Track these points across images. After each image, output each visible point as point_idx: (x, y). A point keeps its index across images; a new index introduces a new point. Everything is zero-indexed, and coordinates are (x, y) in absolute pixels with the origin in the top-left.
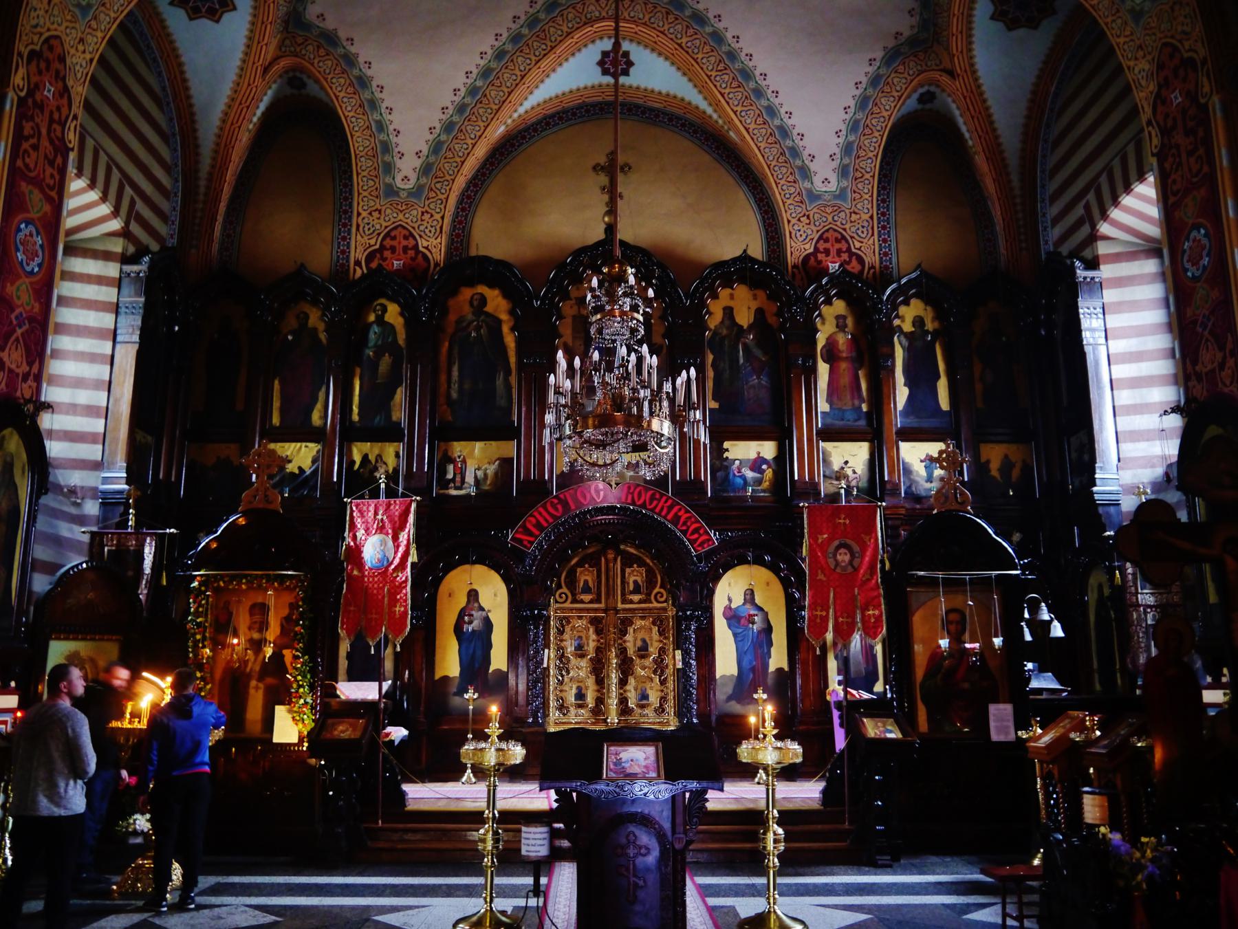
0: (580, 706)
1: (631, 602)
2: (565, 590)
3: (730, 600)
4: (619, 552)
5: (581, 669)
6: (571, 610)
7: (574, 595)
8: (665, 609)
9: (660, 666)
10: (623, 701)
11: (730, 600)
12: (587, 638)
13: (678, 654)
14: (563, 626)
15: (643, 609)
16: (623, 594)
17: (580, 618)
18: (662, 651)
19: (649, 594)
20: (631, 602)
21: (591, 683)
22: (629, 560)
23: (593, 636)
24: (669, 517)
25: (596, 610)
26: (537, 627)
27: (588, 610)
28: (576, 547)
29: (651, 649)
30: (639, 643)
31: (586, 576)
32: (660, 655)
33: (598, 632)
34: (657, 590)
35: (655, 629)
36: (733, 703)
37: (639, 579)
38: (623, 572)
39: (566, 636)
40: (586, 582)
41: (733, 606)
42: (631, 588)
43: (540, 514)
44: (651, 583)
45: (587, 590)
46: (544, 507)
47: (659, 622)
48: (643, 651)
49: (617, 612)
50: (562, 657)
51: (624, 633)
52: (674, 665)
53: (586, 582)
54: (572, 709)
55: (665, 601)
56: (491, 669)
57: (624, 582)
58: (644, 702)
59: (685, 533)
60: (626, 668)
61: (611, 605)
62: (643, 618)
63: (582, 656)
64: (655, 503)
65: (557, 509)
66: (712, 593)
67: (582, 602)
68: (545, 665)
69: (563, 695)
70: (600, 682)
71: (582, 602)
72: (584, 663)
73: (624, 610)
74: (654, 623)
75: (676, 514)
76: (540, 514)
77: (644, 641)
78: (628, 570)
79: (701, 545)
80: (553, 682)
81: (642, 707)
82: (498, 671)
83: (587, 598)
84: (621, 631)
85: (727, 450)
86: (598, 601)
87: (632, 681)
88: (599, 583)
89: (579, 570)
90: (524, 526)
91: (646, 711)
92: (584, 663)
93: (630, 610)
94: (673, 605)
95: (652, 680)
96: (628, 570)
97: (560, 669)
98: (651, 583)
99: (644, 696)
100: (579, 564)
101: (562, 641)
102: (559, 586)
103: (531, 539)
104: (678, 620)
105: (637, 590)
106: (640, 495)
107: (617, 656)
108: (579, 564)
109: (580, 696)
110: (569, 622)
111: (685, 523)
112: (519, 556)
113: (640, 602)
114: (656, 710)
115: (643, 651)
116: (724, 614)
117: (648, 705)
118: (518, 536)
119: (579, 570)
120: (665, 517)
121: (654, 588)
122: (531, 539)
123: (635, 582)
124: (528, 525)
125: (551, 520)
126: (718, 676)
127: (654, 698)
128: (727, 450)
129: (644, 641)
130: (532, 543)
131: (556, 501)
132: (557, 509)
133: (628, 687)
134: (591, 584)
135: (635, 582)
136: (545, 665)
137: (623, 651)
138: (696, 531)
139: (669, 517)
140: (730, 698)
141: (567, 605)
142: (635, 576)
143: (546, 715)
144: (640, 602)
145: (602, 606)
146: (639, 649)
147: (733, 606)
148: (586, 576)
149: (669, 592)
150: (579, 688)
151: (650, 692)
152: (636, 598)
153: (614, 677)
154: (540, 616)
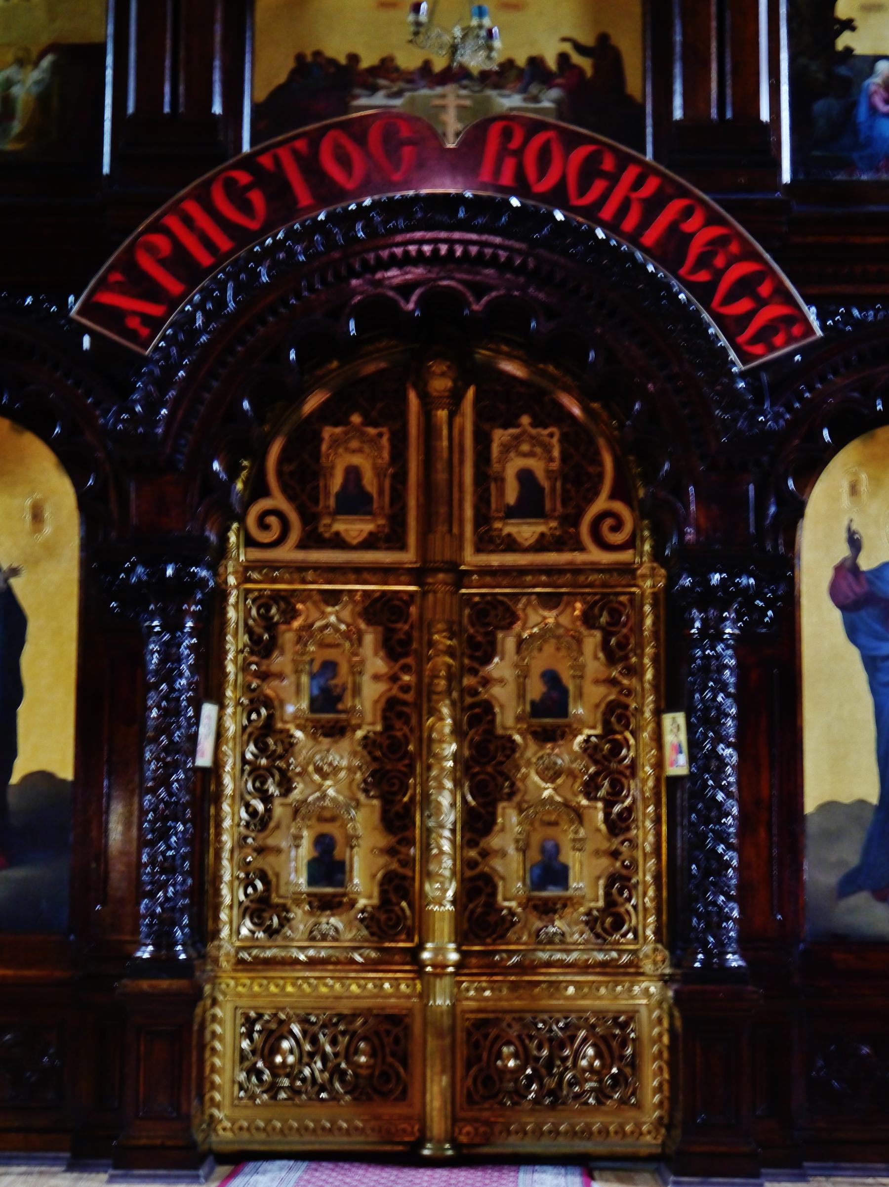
0: (326, 904)
1: (511, 545)
2: (278, 500)
3: (855, 543)
4: (468, 373)
5: (331, 772)
6: (300, 570)
7: (309, 518)
8: (628, 571)
9: (608, 768)
10: (477, 887)
11: (855, 543)
12: (357, 670)
13: (675, 727)
14: (270, 626)
15: (550, 570)
16: (482, 519)
17: (332, 598)
18: (616, 716)
19: (572, 520)
20: (511, 545)
21: (364, 823)
22: (501, 405)
23: (377, 664)
24: (650, 237)
25: (386, 573)
26: (173, 625)
27: (359, 572)
28: (322, 345)
29: (578, 710)
30: (536, 689)
31: (354, 457)
32: (608, 730)
33: (393, 648)
34: (601, 504)
35: (592, 641)
36: (862, 899)
37: (537, 466)
38: (482, 440)
39: (280, 661)
40: (353, 474)
41: (866, 563)
42: (511, 496)
43: (188, 221)
44: (578, 480)
45: (354, 501)
46: (203, 198)
47: (607, 612)
48: (550, 712)
49: (461, 578)
50: (265, 733)
51: (485, 651)
52: (659, 765)
53: (353, 474)
54: (299, 916)
55: (630, 544)
56: (20, 770)
57: (486, 478)
58: (551, 892)
59: (704, 293)
60: (489, 774)
61: (441, 551)
62: (550, 601)
63: (336, 731)
64: (599, 186)
65: (246, 208)
66: (794, 510)
67: (338, 543)
68: (204, 759)
69: (269, 863)
70: (401, 821)
71: (338, 543)
72: (341, 756)
73: (486, 572)
74: (588, 620)
75: (673, 228)
76: (188, 221)
77: (552, 678)
78: (500, 436)
79: (764, 336)
80: (231, 817)
81: (548, 910)
82: (42, 779)
83: (355, 528)
84: (473, 644)
85: (849, 25)
86: (393, 538)
87: (509, 818)
88: (400, 479)
89: (328, 432)
90: (128, 265)
91: (559, 925)
92: (341, 756)
93: (504, 572)
94: (657, 555)
95: (579, 816)
96: (500, 436)
97: (259, 775)
98: (578, 480)
99: (550, 872)
100: (330, 414)
101: (264, 676)
102: (257, 489)
103: (155, 310)
104: (673, 607)
105: (530, 505)
106: (544, 159)
107: (458, 732)
108: (330, 414)
109: (328, 867)
110: (290, 614)
111: (704, 261)
112: (113, 370)
113: (541, 545)
114: (591, 922)
115: (550, 712)
116: (835, 592)
117: (567, 903)
118: (108, 298)
119: (328, 432)
120: (634, 239)
121: (590, 501)
122: (155, 310)
123: (525, 477)
124: (146, 262)
125: (224, 244)
126: (810, 805)
127: (585, 879)
128: (849, 25)
129: (552, 678)
130: (155, 324)
131: (243, 178)
132: (246, 208)
133: (495, 841)
134: (369, 481)
135: (525, 477)
136: (204, 759)
137: (477, 717)
138: (745, 287)
139: (650, 237)
140: (850, 884)
141: (287, 553)
142: (525, 457)
143: (204, 932)
144: (541, 545)
145: (408, 557)
146: (538, 709)
147: (866, 563)
148: (354, 457)
149: (642, 511)
150: (324, 844)
151: (572, 858)
152: (527, 531)
153: (447, 803)
154: (186, 586)
